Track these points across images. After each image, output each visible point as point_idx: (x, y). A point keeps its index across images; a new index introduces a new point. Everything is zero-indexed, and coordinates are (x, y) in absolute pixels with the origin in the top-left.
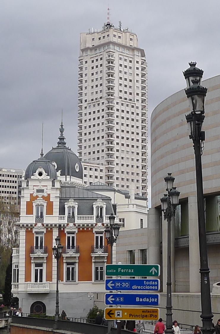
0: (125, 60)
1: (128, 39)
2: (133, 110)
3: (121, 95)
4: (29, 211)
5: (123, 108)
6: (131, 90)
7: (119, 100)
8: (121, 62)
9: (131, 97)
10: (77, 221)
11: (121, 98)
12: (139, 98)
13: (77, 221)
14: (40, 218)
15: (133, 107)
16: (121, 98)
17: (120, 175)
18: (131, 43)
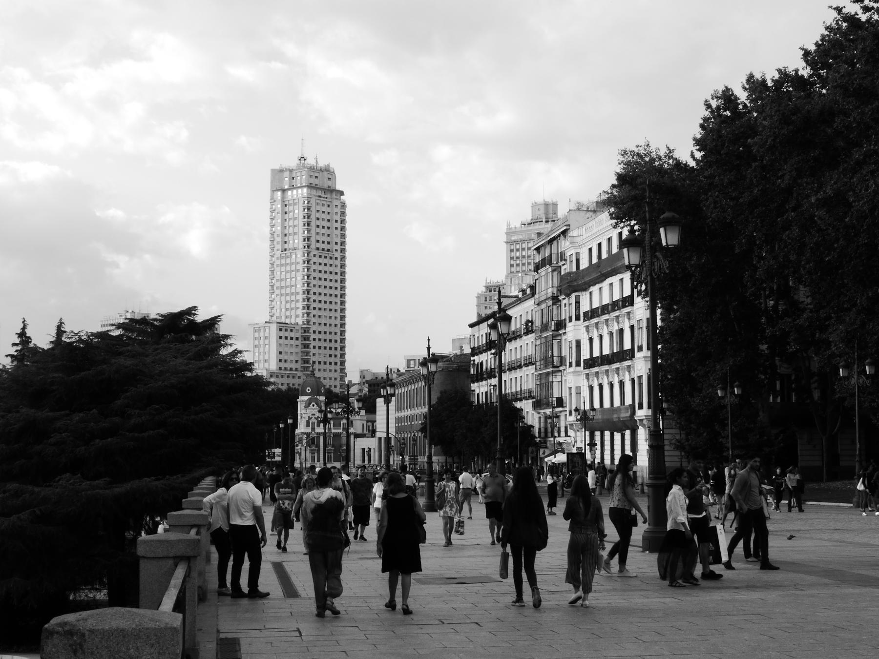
0: (323, 205)
1: (326, 179)
2: (331, 262)
3: (318, 245)
4: (308, 425)
5: (321, 260)
6: (328, 239)
7: (316, 252)
8: (318, 208)
9: (328, 247)
10: (333, 431)
11: (318, 249)
12: (338, 247)
13: (333, 431)
14: (313, 429)
15: (331, 258)
16: (318, 249)
17: (317, 336)
18: (330, 183)
